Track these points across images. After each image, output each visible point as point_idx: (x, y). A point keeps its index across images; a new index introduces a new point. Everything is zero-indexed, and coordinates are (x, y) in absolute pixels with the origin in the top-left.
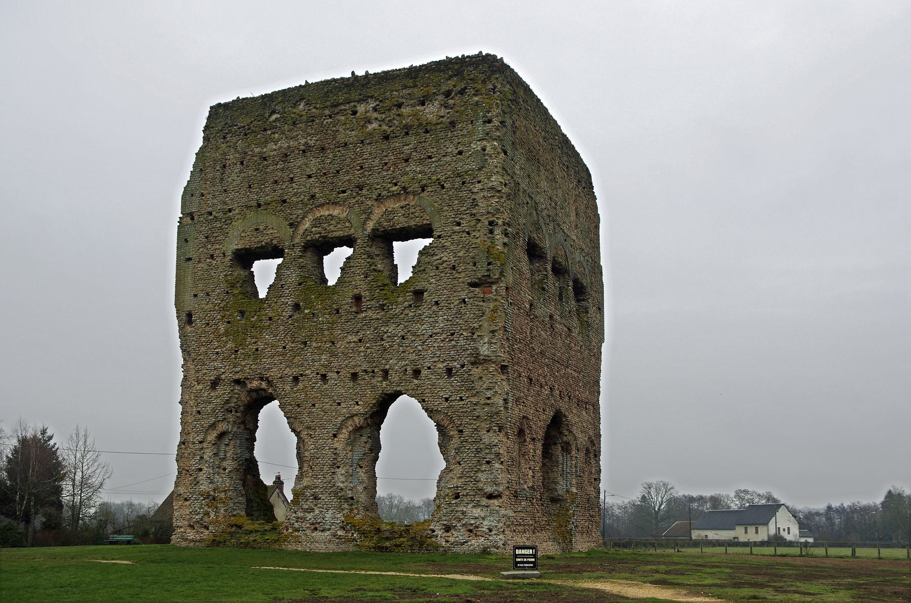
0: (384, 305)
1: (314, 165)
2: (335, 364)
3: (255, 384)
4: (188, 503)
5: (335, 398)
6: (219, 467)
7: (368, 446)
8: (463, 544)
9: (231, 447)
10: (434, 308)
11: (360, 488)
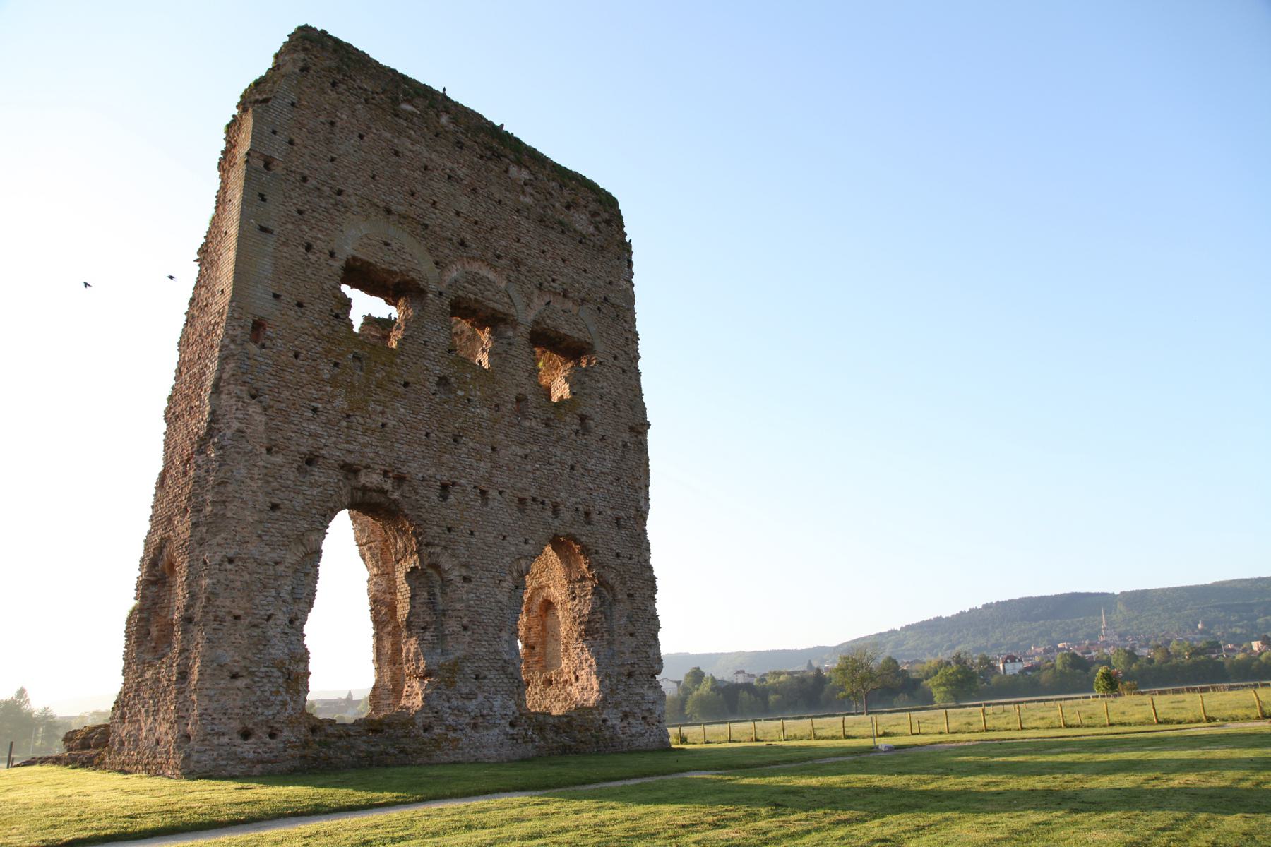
0: (548, 419)
3: (374, 479)
4: (240, 683)
5: (500, 528)
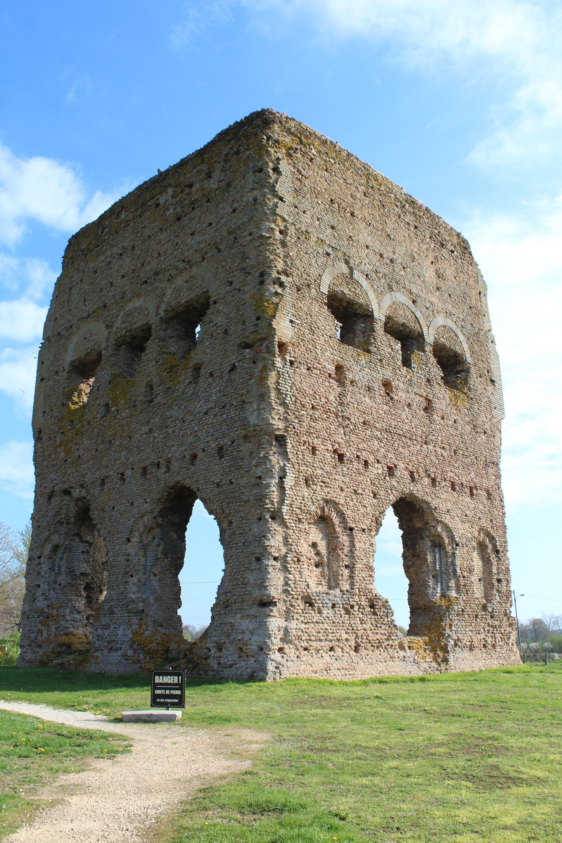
1: (127, 264)
2: (131, 460)
5: (129, 498)
6: (55, 582)
7: (160, 549)
8: (231, 666)
9: (64, 561)
10: (210, 380)
11: (152, 600)
